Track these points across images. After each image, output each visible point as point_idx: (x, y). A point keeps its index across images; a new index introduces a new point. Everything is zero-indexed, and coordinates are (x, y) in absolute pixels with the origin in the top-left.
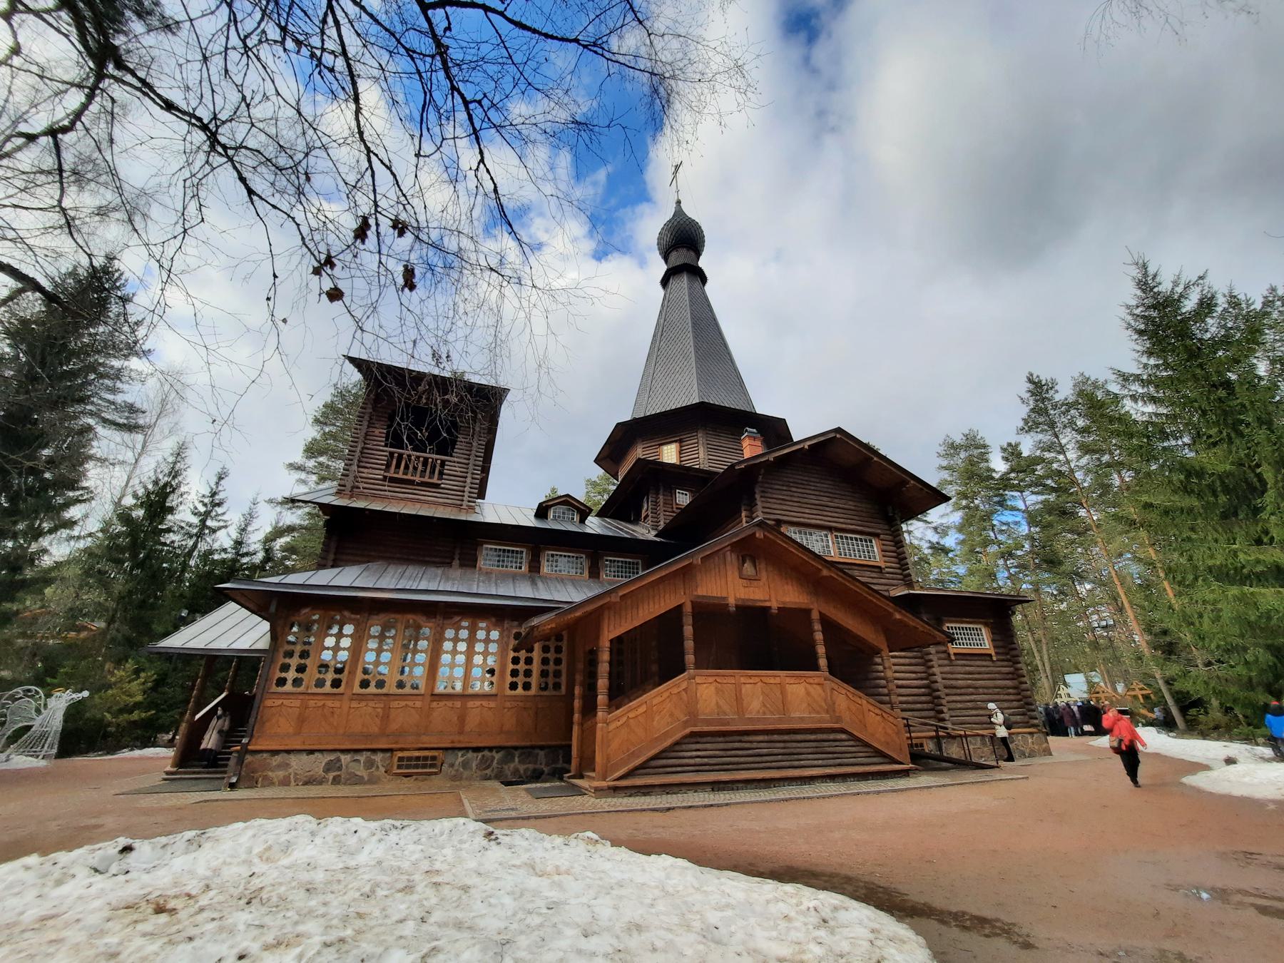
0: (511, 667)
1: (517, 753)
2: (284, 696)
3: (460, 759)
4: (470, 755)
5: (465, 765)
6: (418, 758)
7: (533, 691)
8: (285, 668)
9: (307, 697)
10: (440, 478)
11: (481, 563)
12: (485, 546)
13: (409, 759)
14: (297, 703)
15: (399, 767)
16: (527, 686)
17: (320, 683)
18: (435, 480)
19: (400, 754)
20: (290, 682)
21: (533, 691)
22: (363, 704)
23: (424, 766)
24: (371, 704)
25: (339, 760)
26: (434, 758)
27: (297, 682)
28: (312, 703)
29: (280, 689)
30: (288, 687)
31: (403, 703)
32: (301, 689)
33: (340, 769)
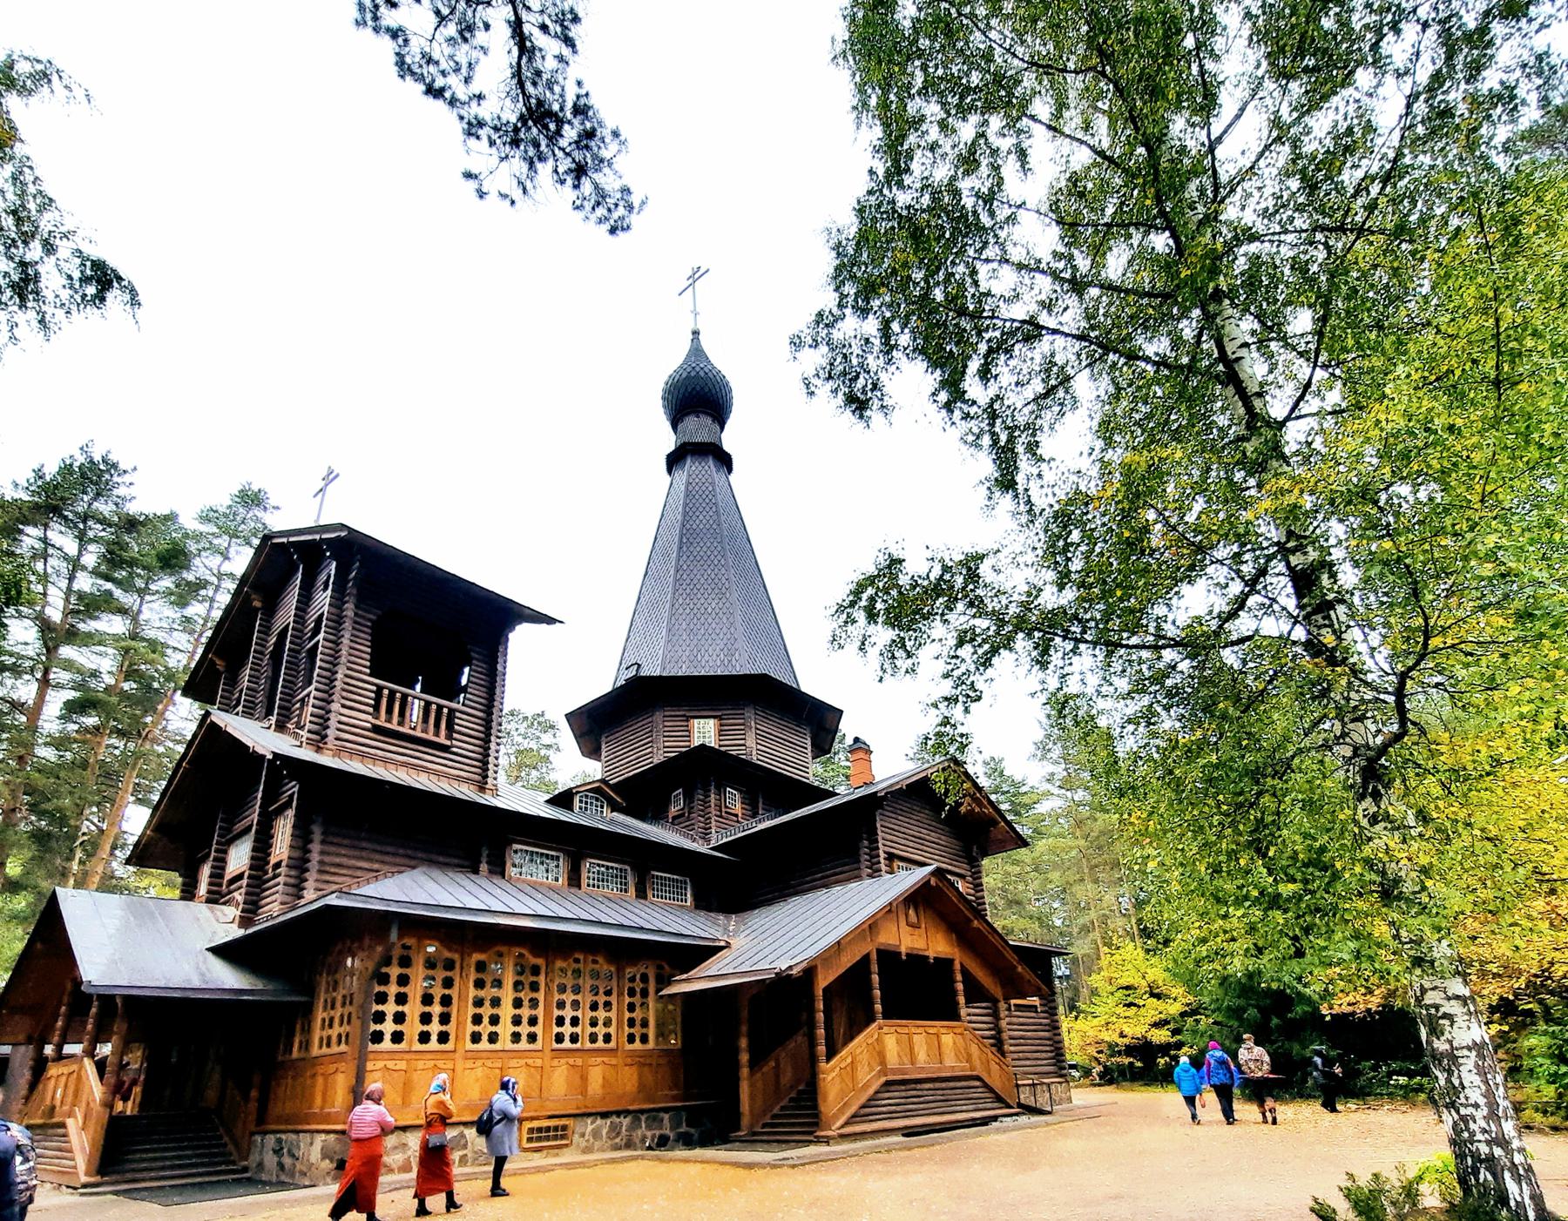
0: (627, 1015)
1: (643, 1118)
2: (386, 1056)
3: (590, 1128)
4: (599, 1121)
5: (596, 1134)
6: (548, 1129)
7: (651, 1045)
8: (380, 1017)
9: (413, 1056)
10: (449, 737)
11: (512, 872)
12: (516, 846)
13: (540, 1130)
14: (402, 1065)
15: (530, 1140)
16: (644, 1039)
17: (424, 1038)
18: (442, 740)
19: (536, 1124)
20: (388, 1037)
21: (651, 1045)
22: (479, 1063)
23: (556, 1138)
24: (489, 1063)
25: (462, 1135)
26: (564, 1128)
27: (397, 1037)
28: (420, 1064)
29: (377, 1047)
30: (387, 1044)
31: (522, 1062)
32: (403, 1046)
33: (465, 1146)
